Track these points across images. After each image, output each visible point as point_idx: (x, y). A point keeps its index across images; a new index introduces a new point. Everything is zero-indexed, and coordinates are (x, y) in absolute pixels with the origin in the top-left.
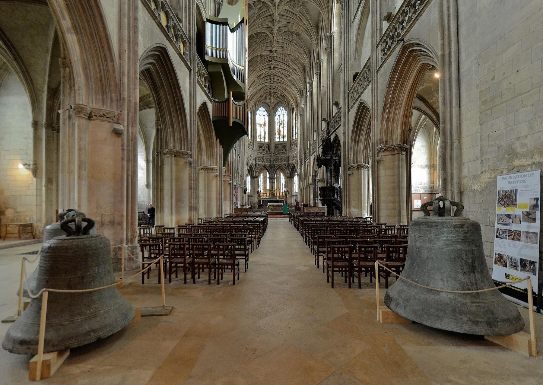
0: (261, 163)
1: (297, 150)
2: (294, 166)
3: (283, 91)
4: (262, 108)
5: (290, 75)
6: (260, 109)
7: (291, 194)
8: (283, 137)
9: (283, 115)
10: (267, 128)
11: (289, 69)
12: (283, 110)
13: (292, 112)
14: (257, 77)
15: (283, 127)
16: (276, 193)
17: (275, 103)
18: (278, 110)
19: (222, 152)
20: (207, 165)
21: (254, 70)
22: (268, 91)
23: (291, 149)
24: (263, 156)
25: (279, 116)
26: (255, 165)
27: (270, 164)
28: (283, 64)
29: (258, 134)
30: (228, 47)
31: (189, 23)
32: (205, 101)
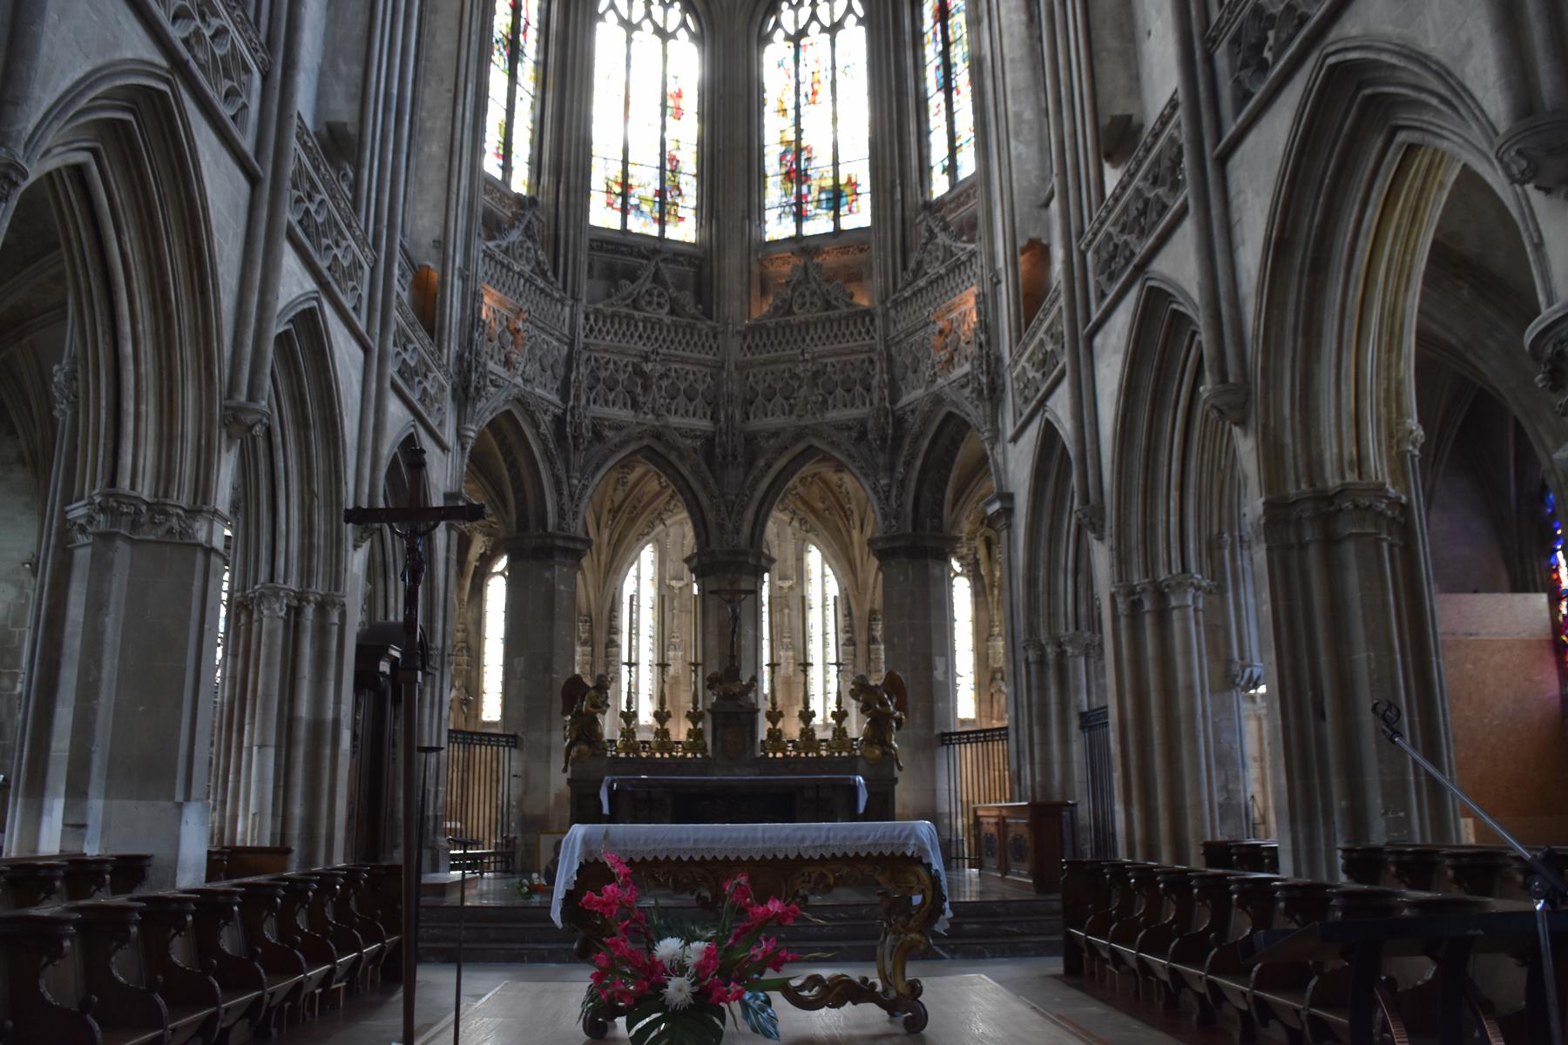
0: (624, 414)
1: (983, 259)
2: (954, 428)
7: (930, 716)
8: (836, 197)
9: (834, 29)
16: (765, 706)
23: (917, 273)
25: (797, 38)
26: (559, 421)
27: (704, 424)
29: (603, 171)
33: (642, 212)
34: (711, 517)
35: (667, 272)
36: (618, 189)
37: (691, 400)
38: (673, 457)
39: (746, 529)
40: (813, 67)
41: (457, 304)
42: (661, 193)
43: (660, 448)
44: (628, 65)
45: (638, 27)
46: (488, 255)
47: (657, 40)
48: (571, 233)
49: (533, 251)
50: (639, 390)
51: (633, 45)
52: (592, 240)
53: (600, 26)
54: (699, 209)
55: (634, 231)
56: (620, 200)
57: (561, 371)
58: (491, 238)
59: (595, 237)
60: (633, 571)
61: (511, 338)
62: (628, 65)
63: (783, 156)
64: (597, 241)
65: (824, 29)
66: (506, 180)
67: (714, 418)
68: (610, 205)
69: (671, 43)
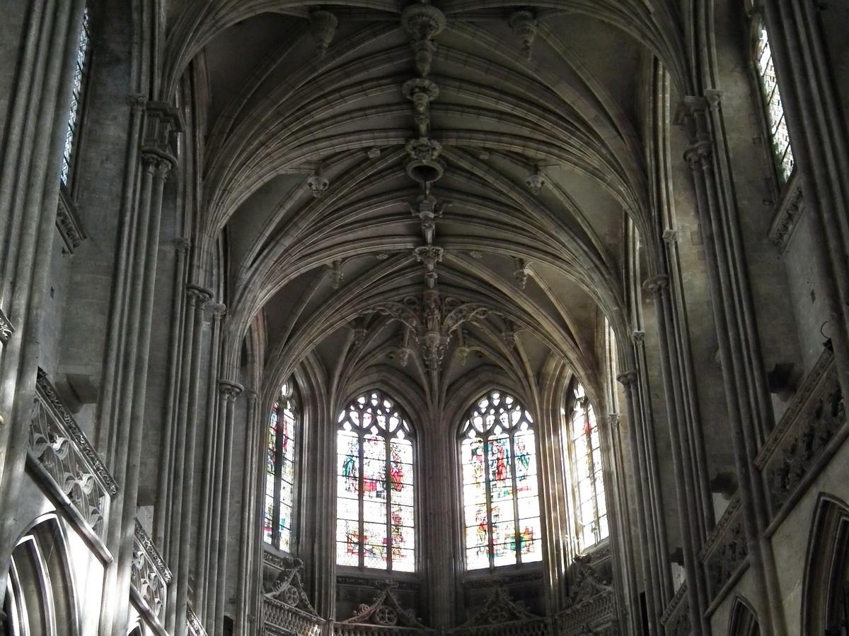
33: (374, 554)
36: (356, 540)
48: (324, 576)
49: (297, 593)
52: (338, 577)
55: (369, 567)
56: (357, 548)
59: (340, 574)
64: (341, 577)
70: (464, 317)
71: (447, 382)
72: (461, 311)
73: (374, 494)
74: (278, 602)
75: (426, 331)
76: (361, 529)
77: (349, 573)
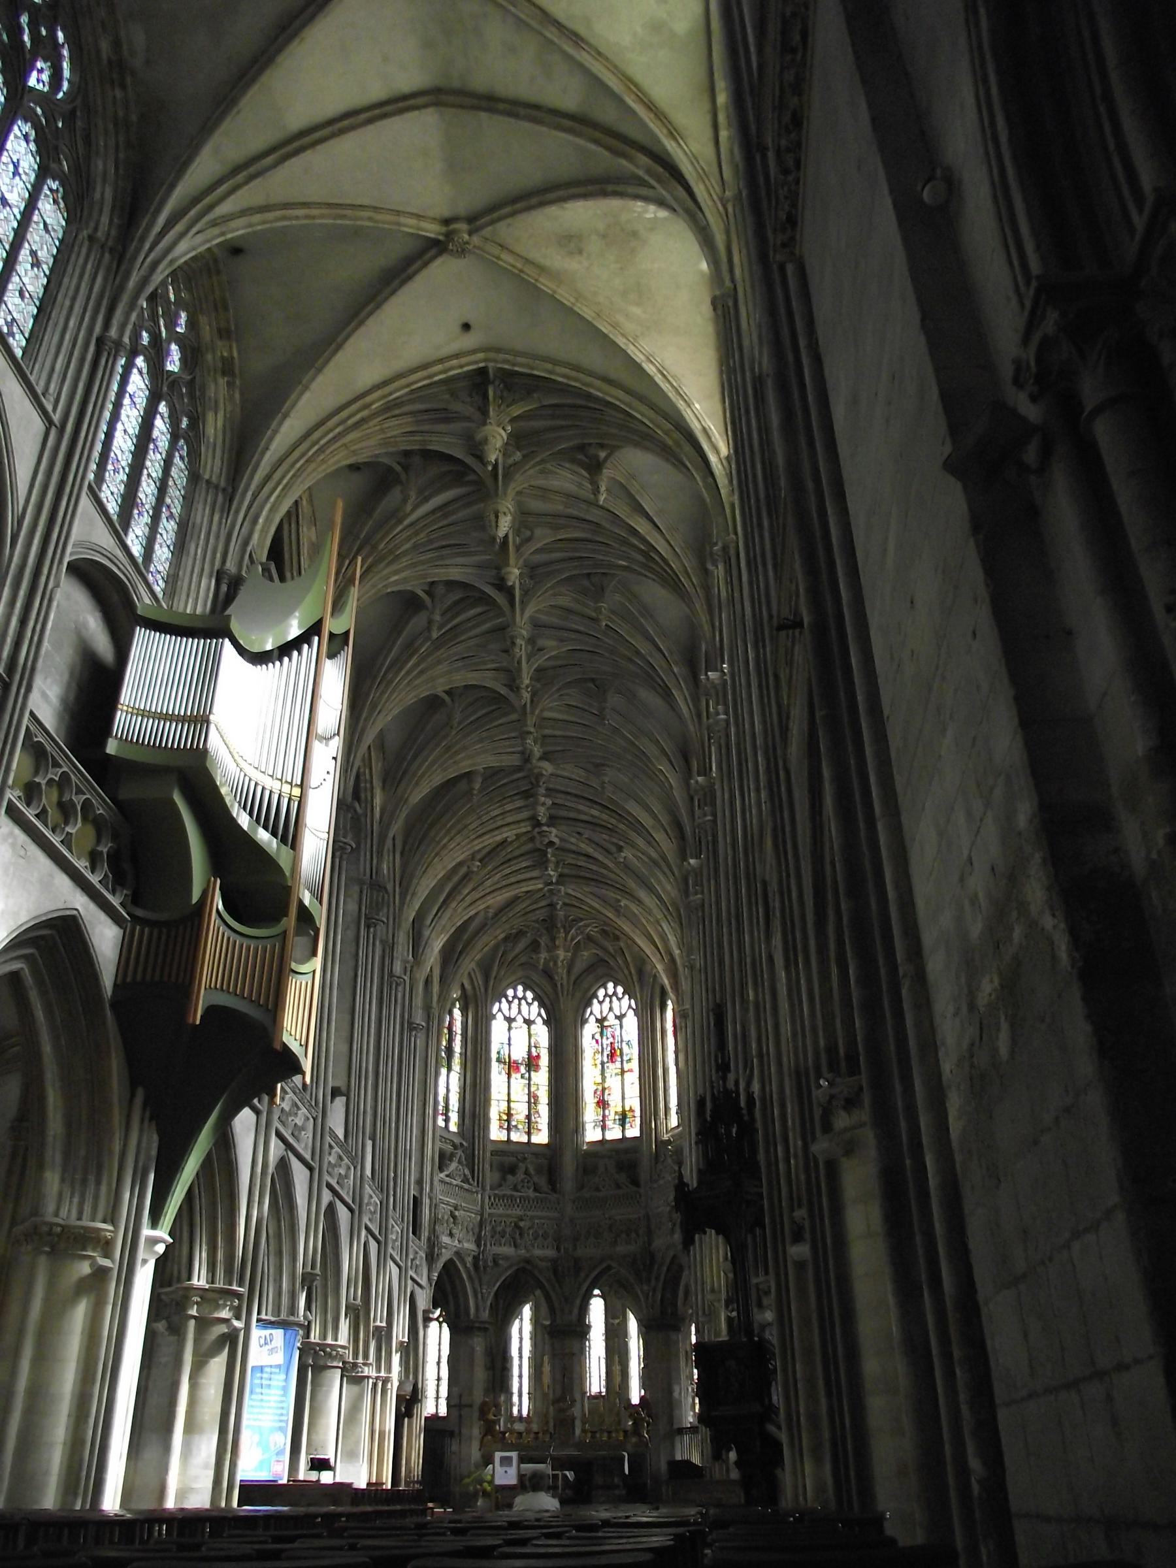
0: (507, 1250)
3: (610, 915)
4: (520, 988)
5: (622, 843)
6: (510, 992)
8: (623, 1119)
9: (620, 1018)
10: (541, 1078)
11: (613, 821)
12: (620, 995)
13: (657, 1003)
14: (479, 856)
15: (623, 1072)
17: (579, 966)
18: (595, 996)
19: (154, 1153)
20: (56, 1215)
21: (460, 826)
22: (541, 914)
24: (519, 1212)
26: (476, 1259)
27: (550, 1253)
28: (588, 803)
29: (496, 1110)
30: (215, 710)
31: (23, 622)
32: (75, 912)
34: (556, 1305)
35: (532, 1171)
36: (505, 1117)
37: (545, 1239)
38: (536, 1272)
39: (576, 1311)
40: (611, 1040)
41: (427, 1212)
42: (528, 1117)
43: (529, 1267)
44: (509, 1044)
45: (514, 1020)
46: (442, 1181)
47: (525, 1026)
50: (517, 1236)
51: (512, 1031)
53: (494, 1022)
54: (550, 1124)
57: (477, 1230)
58: (441, 1169)
60: (517, 1322)
61: (452, 1220)
62: (509, 1044)
63: (595, 1093)
65: (617, 1017)
66: (447, 1126)
67: (558, 1249)
68: (501, 1127)
69: (533, 1027)
70: (582, 933)
71: (573, 978)
72: (579, 928)
73: (519, 1076)
74: (448, 1179)
75: (556, 947)
76: (509, 1108)
77: (501, 1147)
